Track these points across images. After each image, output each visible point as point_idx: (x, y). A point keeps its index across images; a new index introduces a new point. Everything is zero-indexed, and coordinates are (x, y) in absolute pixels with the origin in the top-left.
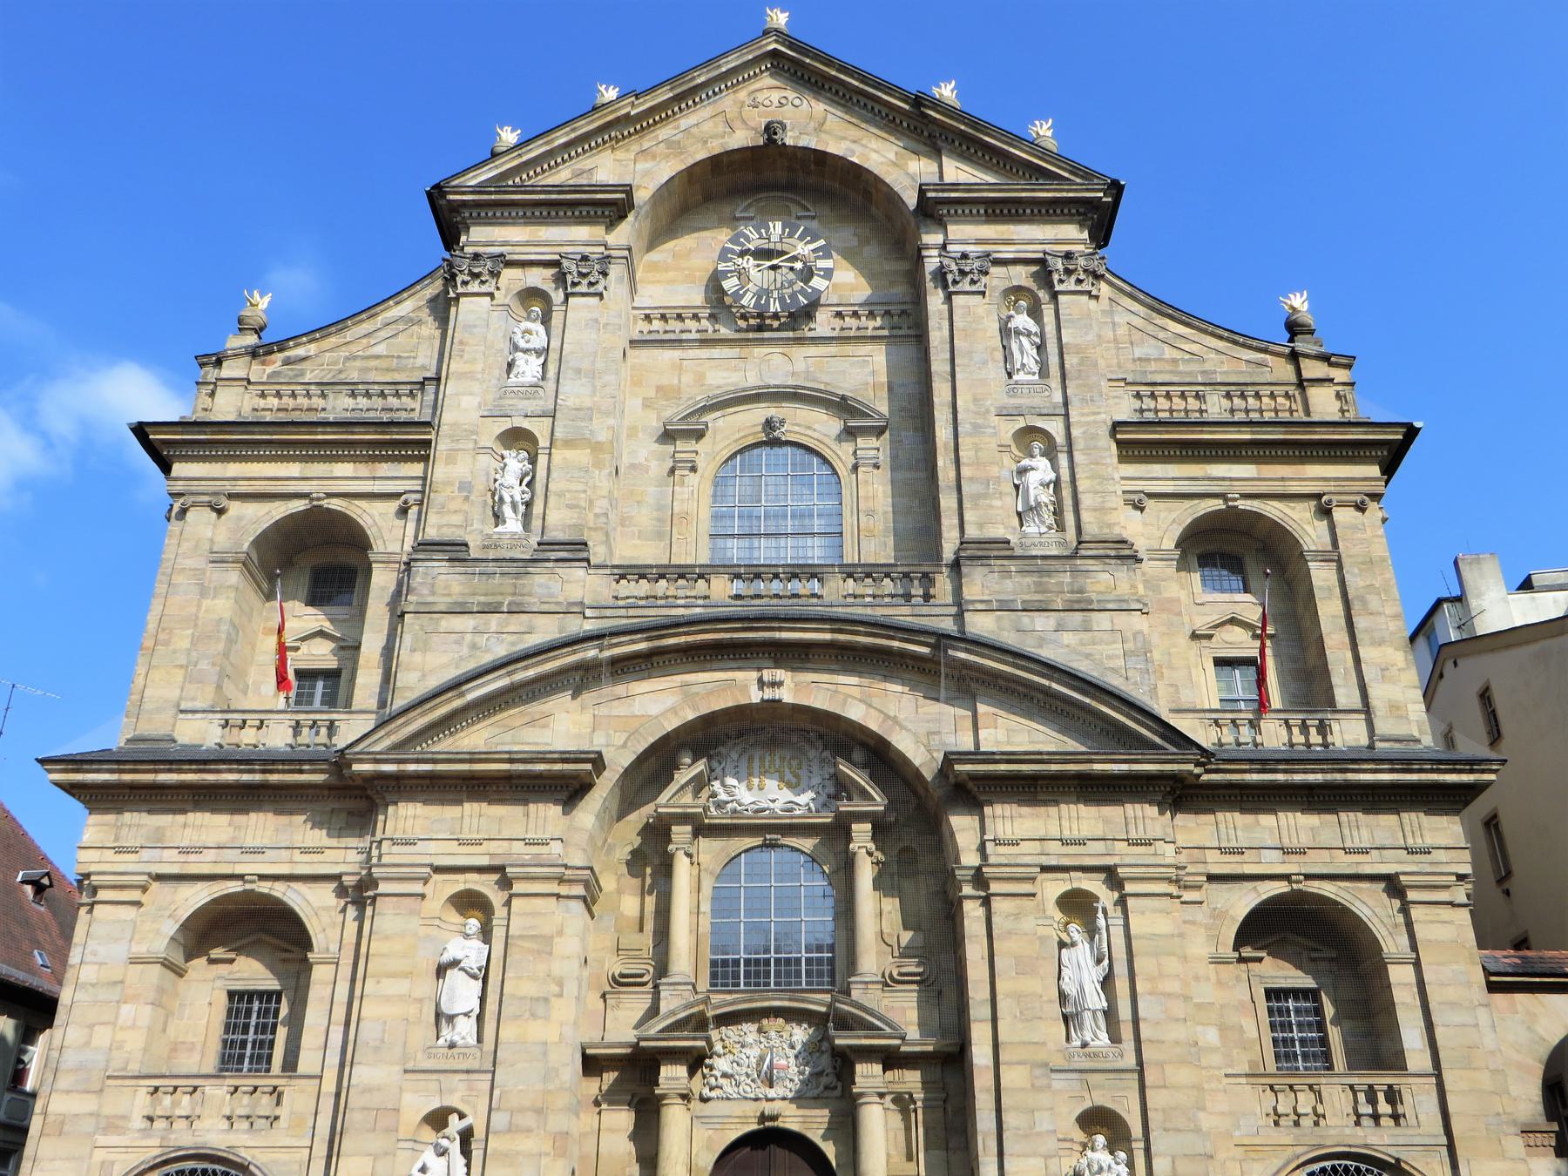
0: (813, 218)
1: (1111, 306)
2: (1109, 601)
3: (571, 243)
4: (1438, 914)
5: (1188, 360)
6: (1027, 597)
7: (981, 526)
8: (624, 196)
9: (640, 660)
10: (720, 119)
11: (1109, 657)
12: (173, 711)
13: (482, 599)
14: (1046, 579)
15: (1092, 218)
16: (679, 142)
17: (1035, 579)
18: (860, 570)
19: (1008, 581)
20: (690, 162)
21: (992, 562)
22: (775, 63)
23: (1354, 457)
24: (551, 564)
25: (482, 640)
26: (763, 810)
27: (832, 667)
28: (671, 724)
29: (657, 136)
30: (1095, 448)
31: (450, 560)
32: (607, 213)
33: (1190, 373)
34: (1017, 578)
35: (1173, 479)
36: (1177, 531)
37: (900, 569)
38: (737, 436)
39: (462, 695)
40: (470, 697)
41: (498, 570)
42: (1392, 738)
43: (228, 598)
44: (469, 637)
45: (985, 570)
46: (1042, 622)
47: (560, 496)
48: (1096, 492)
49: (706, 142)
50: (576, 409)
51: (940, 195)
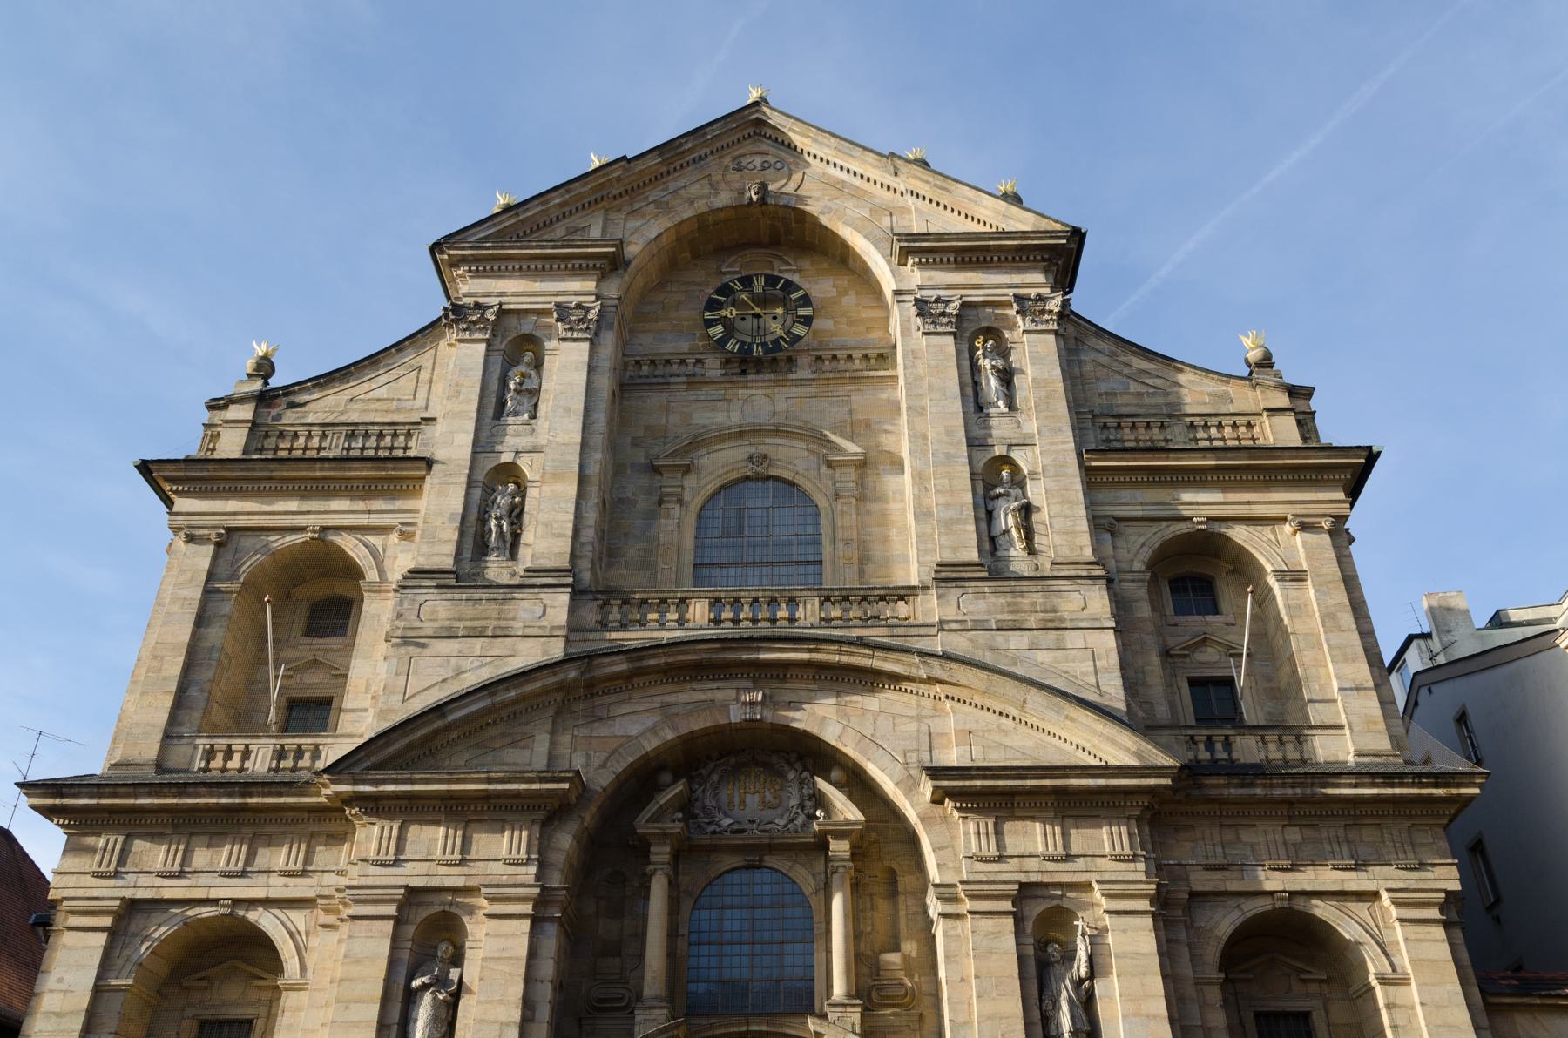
0: (795, 271)
1: (1077, 345)
2: (1082, 620)
3: (564, 294)
4: (1429, 933)
5: (1149, 394)
6: (1000, 617)
7: (955, 549)
8: (614, 249)
9: (621, 681)
10: (706, 181)
11: (1083, 673)
13: (468, 624)
14: (1019, 600)
15: (1057, 264)
16: (667, 203)
17: (1009, 600)
18: (837, 593)
19: (981, 602)
20: (678, 219)
21: (967, 584)
22: (758, 131)
23: (1317, 480)
24: (536, 590)
25: (466, 664)
26: (743, 831)
27: (811, 687)
28: (651, 744)
29: (647, 198)
30: (1065, 475)
31: (437, 587)
32: (598, 266)
33: (1157, 405)
34: (992, 599)
35: (1142, 504)
36: (1146, 553)
37: (876, 593)
38: (721, 471)
39: (444, 716)
40: (450, 718)
41: (484, 596)
42: (1371, 752)
43: (221, 626)
44: (453, 660)
45: (960, 591)
46: (1017, 641)
47: (547, 526)
48: (1066, 517)
49: (692, 203)
50: (564, 444)
51: (912, 244)
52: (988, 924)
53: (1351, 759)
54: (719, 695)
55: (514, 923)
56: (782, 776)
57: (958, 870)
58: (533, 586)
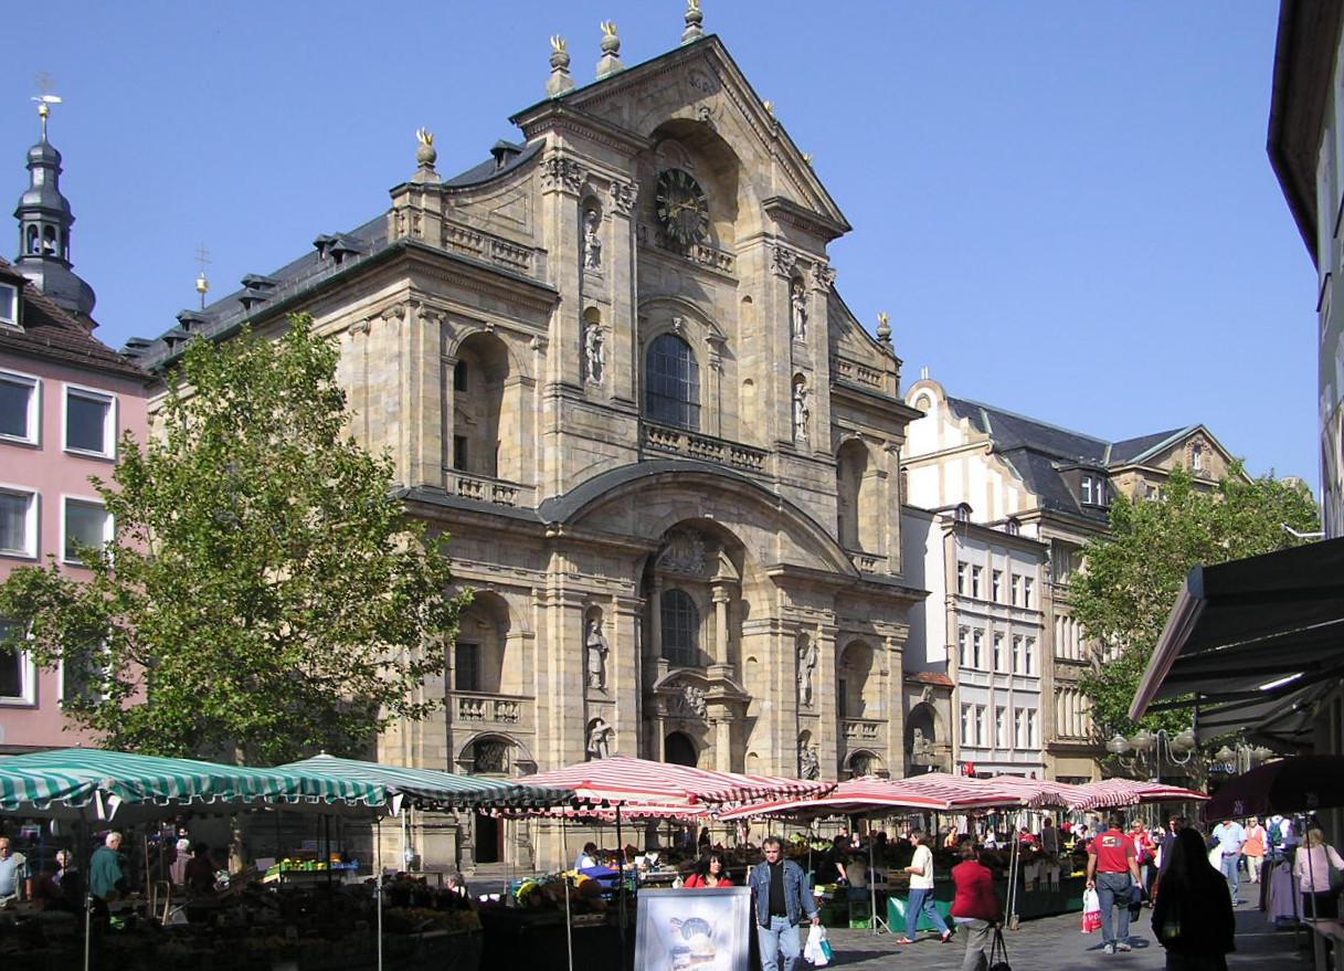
10: (675, 87)
12: (440, 469)
29: (646, 89)
31: (580, 401)
46: (805, 495)
52: (786, 638)
53: (888, 574)
54: (694, 500)
55: (628, 617)
56: (690, 541)
57: (776, 611)
58: (622, 412)
